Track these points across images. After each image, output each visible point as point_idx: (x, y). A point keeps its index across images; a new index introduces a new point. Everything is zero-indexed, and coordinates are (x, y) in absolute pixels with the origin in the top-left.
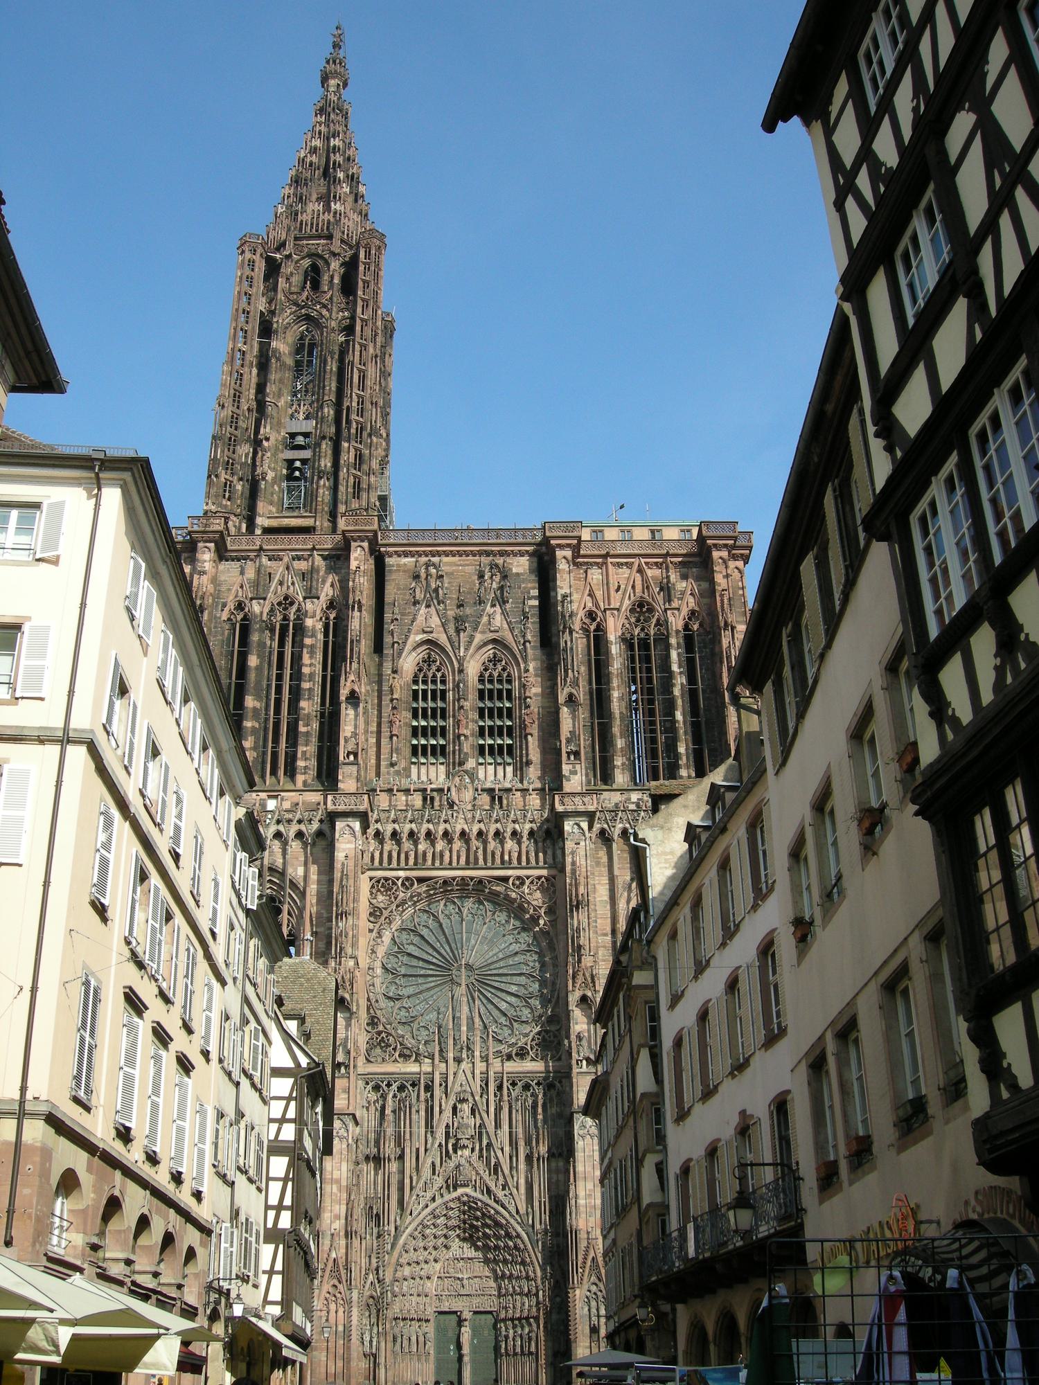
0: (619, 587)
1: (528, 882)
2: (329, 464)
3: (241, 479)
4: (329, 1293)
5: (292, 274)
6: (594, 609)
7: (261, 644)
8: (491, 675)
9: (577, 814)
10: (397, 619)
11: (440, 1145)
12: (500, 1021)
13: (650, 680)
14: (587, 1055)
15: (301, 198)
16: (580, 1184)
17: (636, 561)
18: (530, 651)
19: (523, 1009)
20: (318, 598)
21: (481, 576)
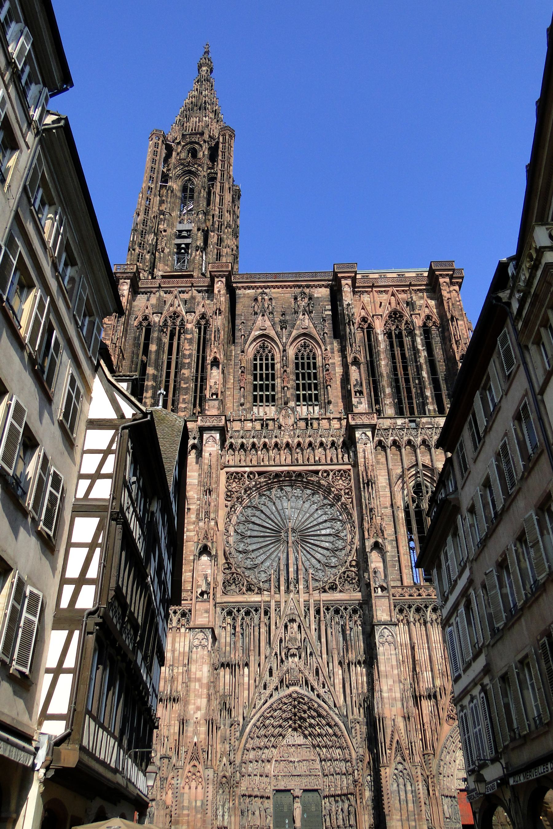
0: (381, 303)
1: (331, 474)
2: (202, 244)
3: (149, 252)
4: (190, 772)
5: (181, 152)
6: (366, 316)
7: (159, 340)
8: (303, 355)
9: (364, 426)
10: (243, 323)
11: (276, 654)
12: (316, 567)
13: (403, 356)
14: (381, 584)
15: (186, 117)
16: (383, 680)
17: (390, 289)
18: (328, 340)
19: (331, 558)
20: (195, 312)
21: (296, 299)
